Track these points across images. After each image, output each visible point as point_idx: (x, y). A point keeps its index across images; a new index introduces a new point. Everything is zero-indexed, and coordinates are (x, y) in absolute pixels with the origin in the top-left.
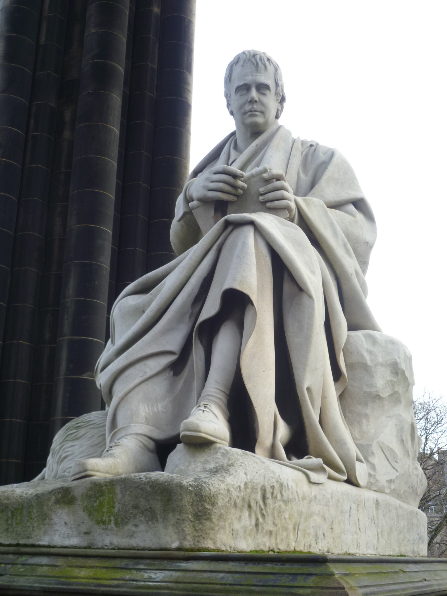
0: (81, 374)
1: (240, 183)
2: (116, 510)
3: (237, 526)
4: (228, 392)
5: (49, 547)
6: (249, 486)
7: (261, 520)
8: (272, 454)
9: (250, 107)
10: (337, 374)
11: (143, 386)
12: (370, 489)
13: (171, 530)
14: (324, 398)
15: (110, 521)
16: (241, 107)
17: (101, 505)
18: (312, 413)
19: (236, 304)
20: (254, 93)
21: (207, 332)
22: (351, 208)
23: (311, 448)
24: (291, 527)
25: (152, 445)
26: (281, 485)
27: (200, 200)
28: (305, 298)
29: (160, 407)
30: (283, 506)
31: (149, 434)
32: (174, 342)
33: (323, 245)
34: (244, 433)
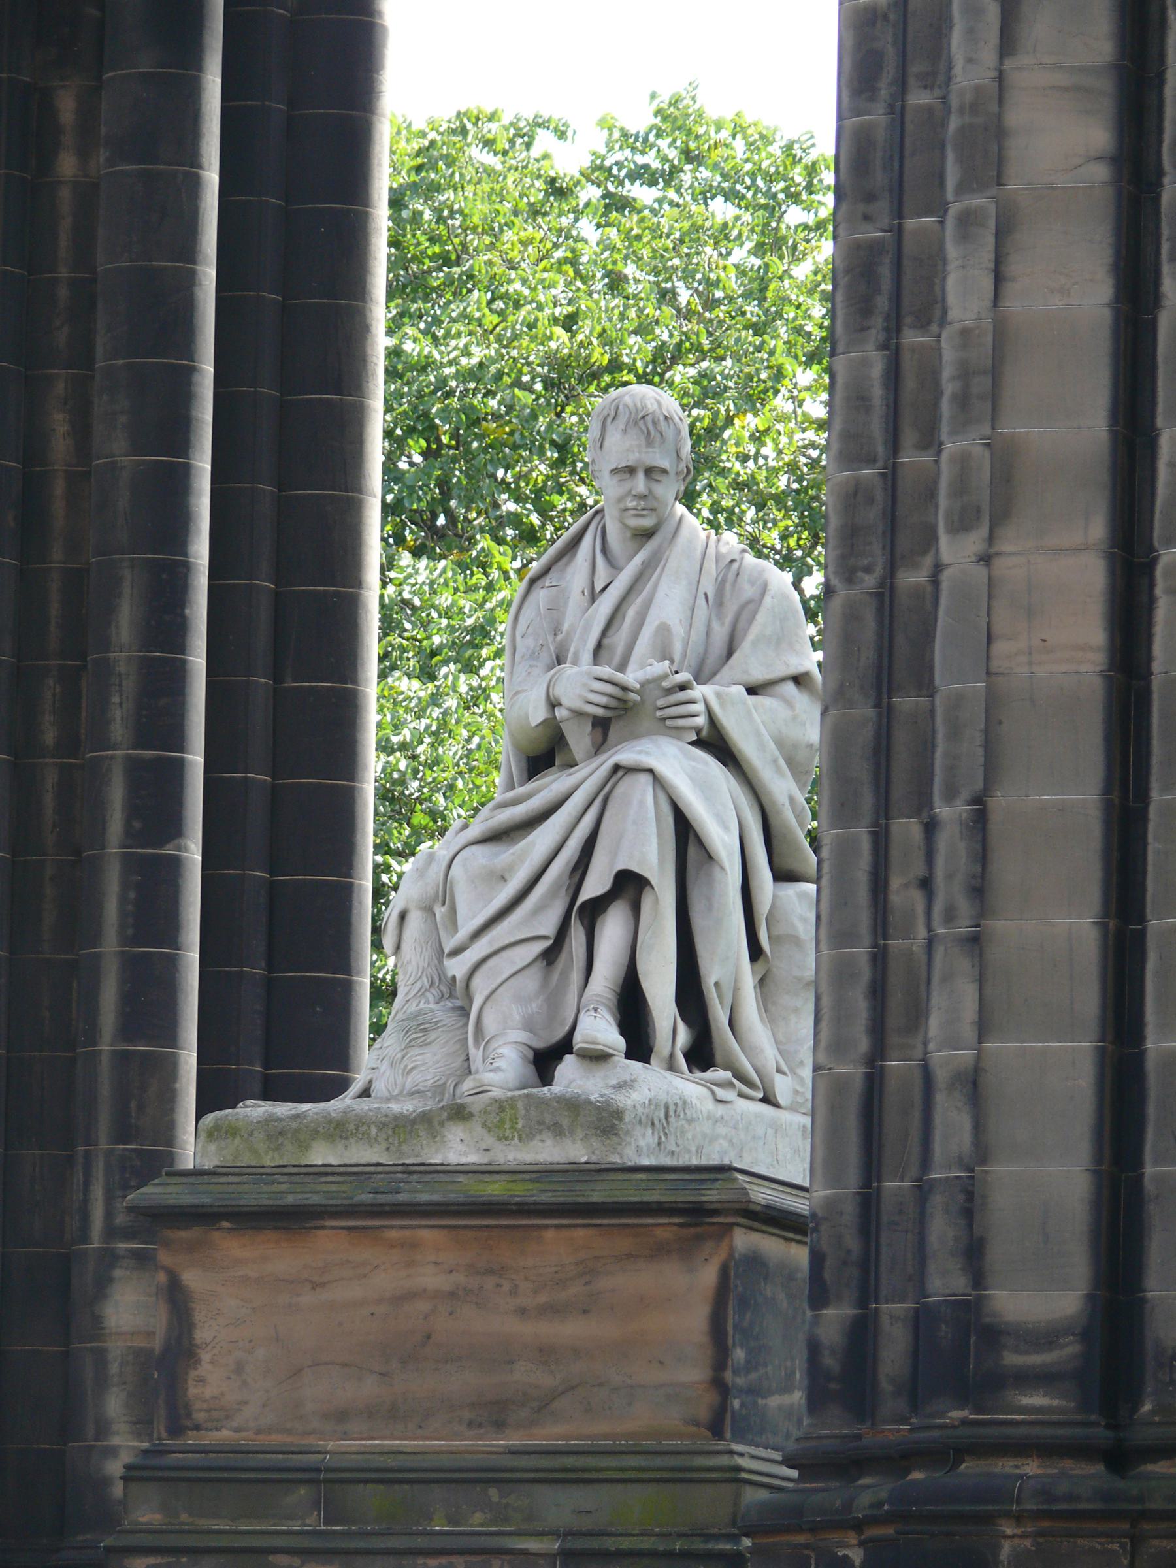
0: (161, 845)
1: (632, 696)
2: (520, 1125)
3: (642, 1143)
4: (618, 991)
5: (442, 1164)
6: (654, 1102)
7: (663, 1139)
8: (671, 1067)
9: (634, 503)
10: (756, 952)
11: (512, 980)
12: (796, 1111)
13: (579, 1145)
14: (736, 990)
15: (513, 1137)
16: (621, 499)
17: (502, 1121)
18: (719, 1015)
19: (629, 885)
20: (640, 483)
21: (593, 911)
22: (790, 687)
23: (719, 1057)
24: (694, 1149)
25: (531, 1055)
26: (685, 1103)
27: (571, 710)
28: (717, 870)
29: (534, 1006)
30: (686, 1126)
31: (529, 1043)
32: (548, 925)
33: (744, 766)
34: (639, 1044)
